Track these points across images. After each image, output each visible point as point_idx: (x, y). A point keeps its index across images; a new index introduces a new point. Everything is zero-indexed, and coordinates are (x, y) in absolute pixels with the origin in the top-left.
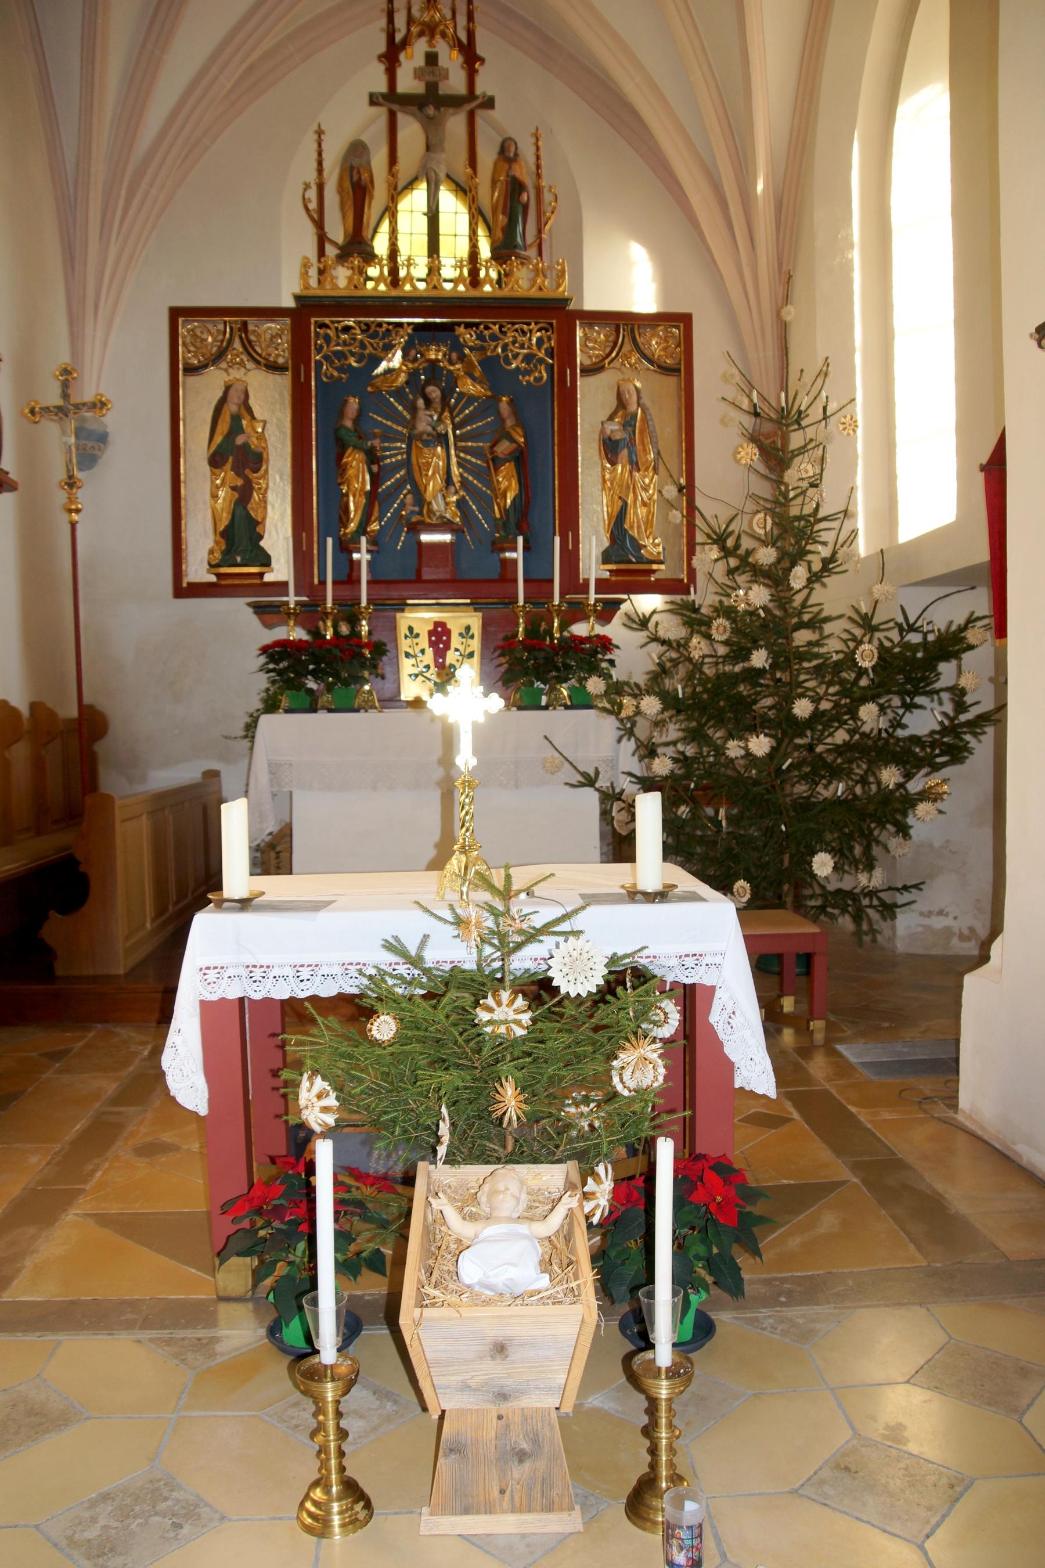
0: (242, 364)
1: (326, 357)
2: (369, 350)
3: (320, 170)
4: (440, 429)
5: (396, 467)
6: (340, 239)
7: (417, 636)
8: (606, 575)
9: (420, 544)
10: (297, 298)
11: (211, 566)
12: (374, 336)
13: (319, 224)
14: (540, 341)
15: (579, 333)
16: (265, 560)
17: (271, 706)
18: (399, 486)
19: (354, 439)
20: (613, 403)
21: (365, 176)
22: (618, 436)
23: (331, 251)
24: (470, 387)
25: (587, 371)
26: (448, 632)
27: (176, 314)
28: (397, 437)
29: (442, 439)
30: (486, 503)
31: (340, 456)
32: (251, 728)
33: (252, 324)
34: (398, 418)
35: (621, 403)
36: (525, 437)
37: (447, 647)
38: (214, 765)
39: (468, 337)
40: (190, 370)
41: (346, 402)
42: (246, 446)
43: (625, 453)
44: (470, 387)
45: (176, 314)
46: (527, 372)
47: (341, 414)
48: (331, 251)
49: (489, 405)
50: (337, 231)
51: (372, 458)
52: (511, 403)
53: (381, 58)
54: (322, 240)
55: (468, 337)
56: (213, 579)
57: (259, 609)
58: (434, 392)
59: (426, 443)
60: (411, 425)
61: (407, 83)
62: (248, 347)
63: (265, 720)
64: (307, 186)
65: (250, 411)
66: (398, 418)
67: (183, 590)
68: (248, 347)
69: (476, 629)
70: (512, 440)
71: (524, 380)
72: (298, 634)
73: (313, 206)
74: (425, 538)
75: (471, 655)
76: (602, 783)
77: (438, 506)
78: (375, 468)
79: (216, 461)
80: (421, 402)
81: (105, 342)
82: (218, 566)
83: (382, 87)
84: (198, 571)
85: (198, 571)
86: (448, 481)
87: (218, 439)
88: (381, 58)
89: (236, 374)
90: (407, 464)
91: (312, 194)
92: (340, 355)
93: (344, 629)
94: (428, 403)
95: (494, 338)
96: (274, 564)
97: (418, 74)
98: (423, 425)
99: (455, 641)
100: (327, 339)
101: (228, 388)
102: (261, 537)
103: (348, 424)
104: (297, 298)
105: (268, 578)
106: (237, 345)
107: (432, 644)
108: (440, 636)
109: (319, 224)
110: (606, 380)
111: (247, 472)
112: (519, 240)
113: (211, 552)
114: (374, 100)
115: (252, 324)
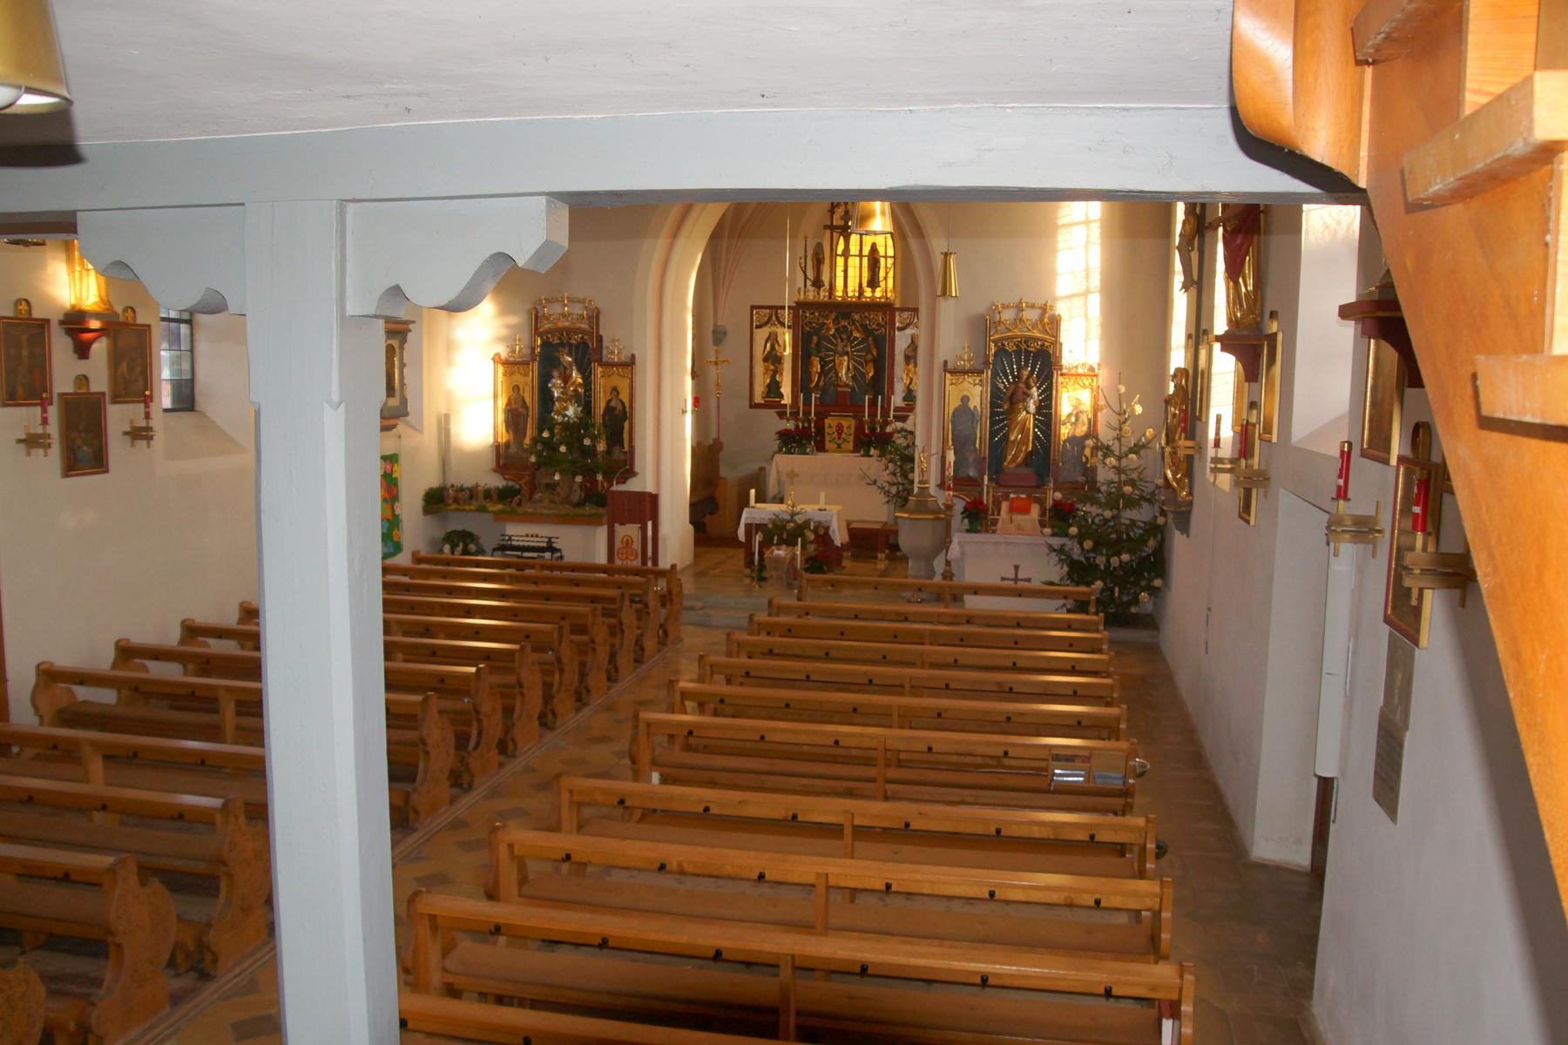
0: (775, 325)
1: (806, 324)
2: (820, 321)
3: (806, 252)
4: (846, 349)
5: (830, 362)
6: (812, 279)
7: (831, 427)
8: (903, 405)
9: (838, 392)
10: (796, 303)
11: (763, 398)
12: (823, 316)
13: (805, 272)
14: (883, 319)
15: (897, 318)
16: (782, 396)
17: (780, 451)
18: (830, 369)
19: (815, 352)
20: (910, 341)
21: (821, 256)
22: (910, 354)
23: (809, 283)
24: (856, 334)
25: (900, 329)
26: (842, 427)
27: (753, 308)
28: (831, 350)
29: (847, 353)
30: (863, 375)
31: (810, 358)
32: (773, 457)
33: (779, 311)
34: (832, 344)
35: (913, 342)
36: (878, 352)
37: (842, 431)
38: (764, 465)
39: (857, 317)
40: (757, 327)
41: (812, 338)
42: (776, 355)
43: (912, 361)
44: (856, 334)
45: (753, 308)
46: (878, 330)
47: (811, 342)
48: (809, 283)
49: (864, 340)
50: (810, 274)
51: (822, 359)
52: (873, 340)
53: (829, 211)
54: (806, 277)
55: (857, 317)
56: (763, 402)
57: (778, 413)
58: (844, 336)
59: (841, 356)
60: (836, 345)
61: (837, 221)
62: (777, 318)
63: (777, 456)
64: (801, 258)
65: (778, 342)
66: (832, 344)
67: (753, 406)
68: (777, 318)
69: (853, 426)
70: (873, 355)
71: (876, 333)
72: (790, 425)
73: (803, 265)
74: (839, 389)
75: (850, 435)
76: (879, 484)
77: (844, 378)
78: (822, 363)
79: (765, 360)
80: (839, 340)
81: (727, 294)
82: (766, 397)
83: (829, 223)
84: (758, 399)
85: (758, 399)
86: (848, 369)
87: (766, 353)
88: (829, 211)
89: (773, 329)
90: (834, 361)
91: (803, 261)
92: (810, 323)
93: (806, 425)
94: (842, 340)
95: (866, 317)
96: (785, 397)
97: (842, 218)
98: (840, 349)
99: (845, 429)
100: (806, 317)
101: (770, 334)
102: (780, 388)
103: (813, 346)
104: (796, 303)
105: (783, 402)
106: (774, 318)
107: (837, 431)
108: (840, 429)
109: (805, 272)
110: (909, 331)
111: (777, 365)
112: (876, 281)
113: (763, 392)
114: (826, 227)
115: (779, 311)
